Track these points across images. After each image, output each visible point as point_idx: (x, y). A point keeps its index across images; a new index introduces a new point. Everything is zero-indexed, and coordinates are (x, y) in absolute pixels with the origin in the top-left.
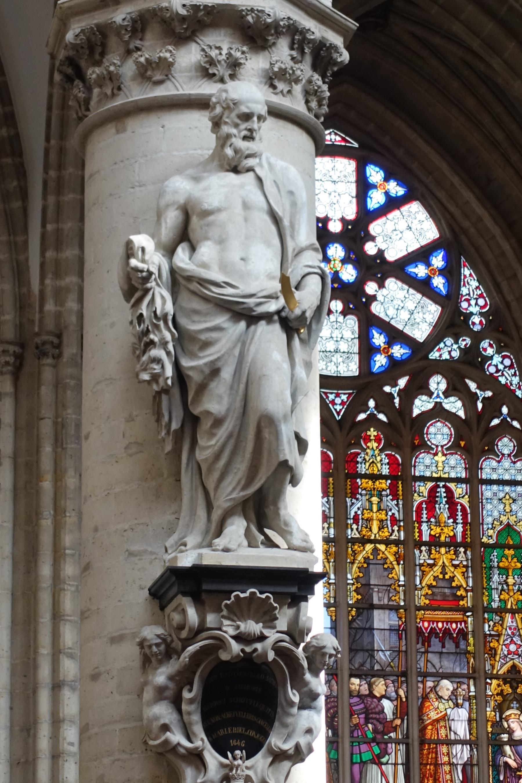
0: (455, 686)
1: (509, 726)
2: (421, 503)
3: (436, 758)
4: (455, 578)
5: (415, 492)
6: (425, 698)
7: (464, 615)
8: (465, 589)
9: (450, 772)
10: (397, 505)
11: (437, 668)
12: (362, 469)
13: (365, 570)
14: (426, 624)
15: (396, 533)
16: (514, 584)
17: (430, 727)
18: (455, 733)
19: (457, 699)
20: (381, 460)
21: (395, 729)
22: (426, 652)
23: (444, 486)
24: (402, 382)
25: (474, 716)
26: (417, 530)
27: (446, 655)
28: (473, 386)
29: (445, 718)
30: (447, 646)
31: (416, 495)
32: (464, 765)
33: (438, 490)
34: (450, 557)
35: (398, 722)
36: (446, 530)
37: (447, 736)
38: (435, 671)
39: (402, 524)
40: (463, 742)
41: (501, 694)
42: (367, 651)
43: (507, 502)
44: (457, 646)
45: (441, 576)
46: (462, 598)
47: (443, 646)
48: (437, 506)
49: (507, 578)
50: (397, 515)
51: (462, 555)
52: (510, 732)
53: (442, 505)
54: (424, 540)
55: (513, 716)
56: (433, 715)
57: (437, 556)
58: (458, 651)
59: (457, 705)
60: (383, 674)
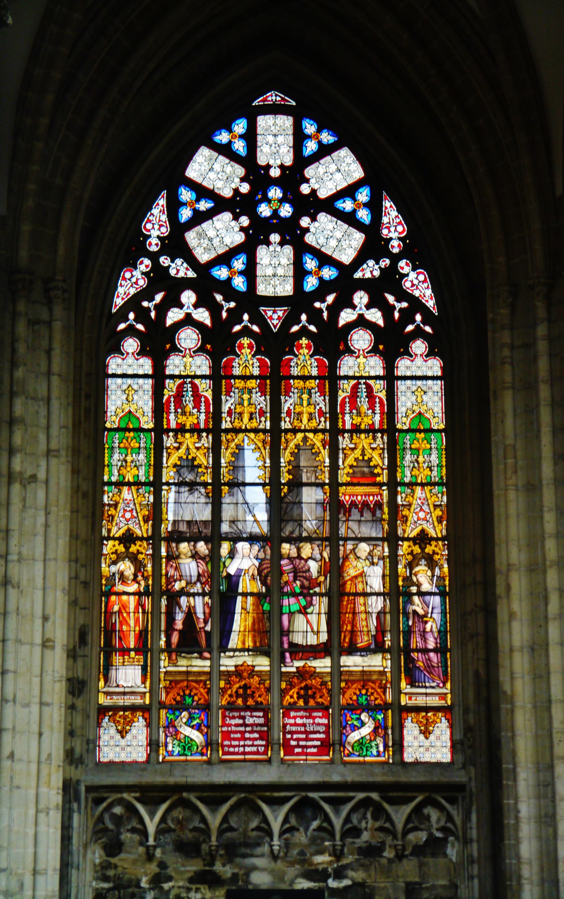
0: (372, 548)
1: (417, 580)
2: (345, 398)
3: (354, 607)
4: (373, 459)
5: (340, 388)
6: (346, 558)
7: (380, 488)
8: (381, 468)
9: (366, 619)
10: (324, 400)
11: (357, 533)
12: (295, 371)
13: (296, 455)
14: (347, 498)
15: (323, 423)
16: (424, 462)
17: (349, 583)
18: (371, 587)
19: (372, 559)
20: (311, 364)
21: (319, 585)
22: (348, 520)
23: (364, 383)
24: (330, 299)
25: (387, 572)
26: (340, 420)
27: (364, 523)
28: (391, 299)
29: (362, 574)
30: (365, 515)
31: (340, 391)
32: (379, 613)
33: (360, 386)
34: (368, 441)
35: (322, 579)
36: (365, 419)
37: (364, 589)
38: (354, 536)
39: (328, 415)
40: (377, 594)
41: (411, 553)
42: (296, 521)
43: (419, 394)
44: (374, 514)
45: (361, 458)
46: (378, 475)
47: (362, 515)
48: (358, 400)
49: (418, 457)
50: (323, 409)
51: (379, 441)
52: (419, 585)
53: (362, 399)
54: (347, 428)
55: (421, 572)
56: (352, 572)
57: (358, 441)
58: (375, 518)
59: (373, 564)
60: (310, 539)
